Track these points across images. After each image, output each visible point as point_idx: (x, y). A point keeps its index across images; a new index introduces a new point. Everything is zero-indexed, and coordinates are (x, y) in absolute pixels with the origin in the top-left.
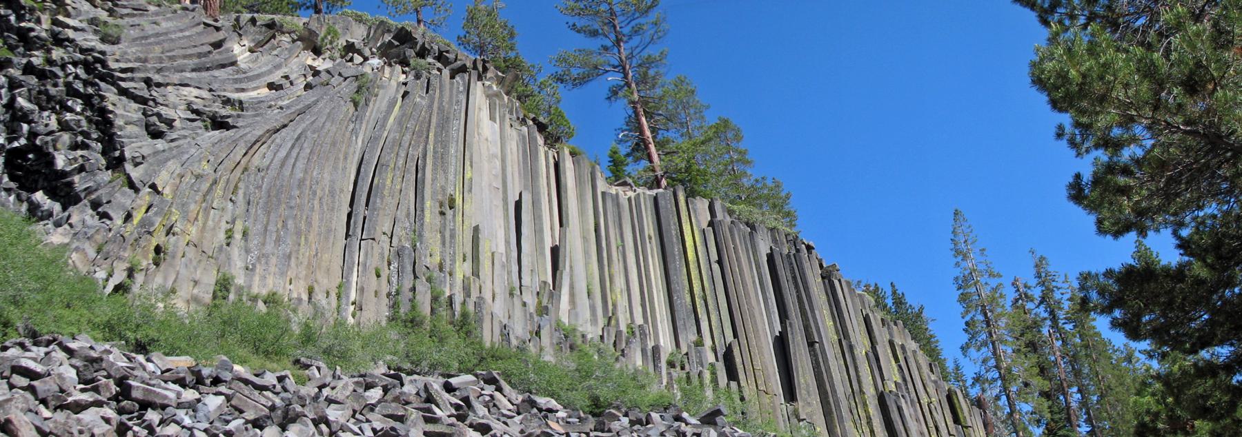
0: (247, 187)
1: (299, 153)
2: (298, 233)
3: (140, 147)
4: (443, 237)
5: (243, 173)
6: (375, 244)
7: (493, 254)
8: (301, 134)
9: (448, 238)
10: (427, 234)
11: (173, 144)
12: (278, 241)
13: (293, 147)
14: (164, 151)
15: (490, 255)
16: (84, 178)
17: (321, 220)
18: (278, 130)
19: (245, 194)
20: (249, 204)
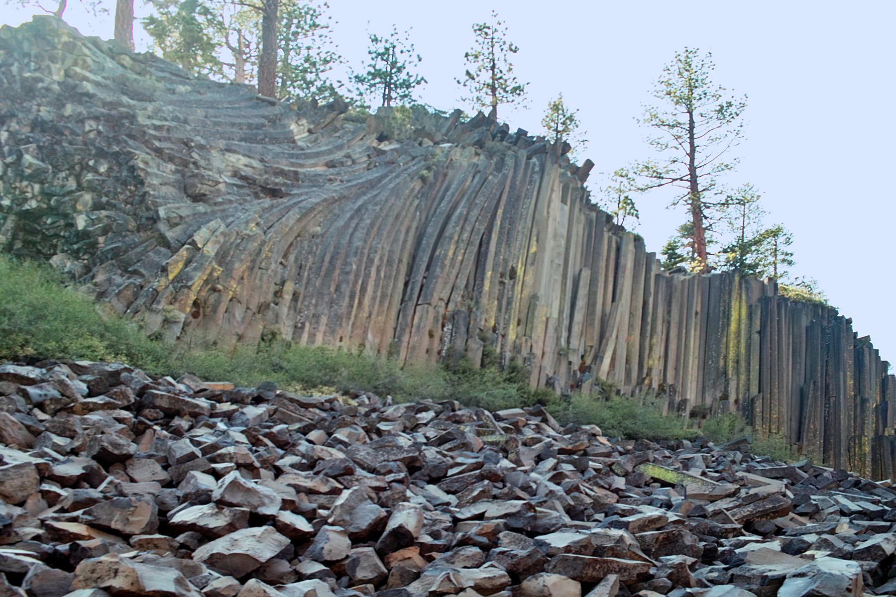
0: (300, 252)
1: (358, 224)
2: (352, 297)
3: (178, 208)
4: (500, 304)
5: (296, 238)
6: (431, 309)
7: (547, 319)
8: (362, 205)
9: (505, 303)
10: (484, 300)
11: (216, 208)
12: (332, 303)
13: (352, 218)
14: (206, 213)
15: (544, 319)
16: (112, 239)
17: (376, 285)
18: (336, 200)
19: (296, 259)
20: (300, 267)
